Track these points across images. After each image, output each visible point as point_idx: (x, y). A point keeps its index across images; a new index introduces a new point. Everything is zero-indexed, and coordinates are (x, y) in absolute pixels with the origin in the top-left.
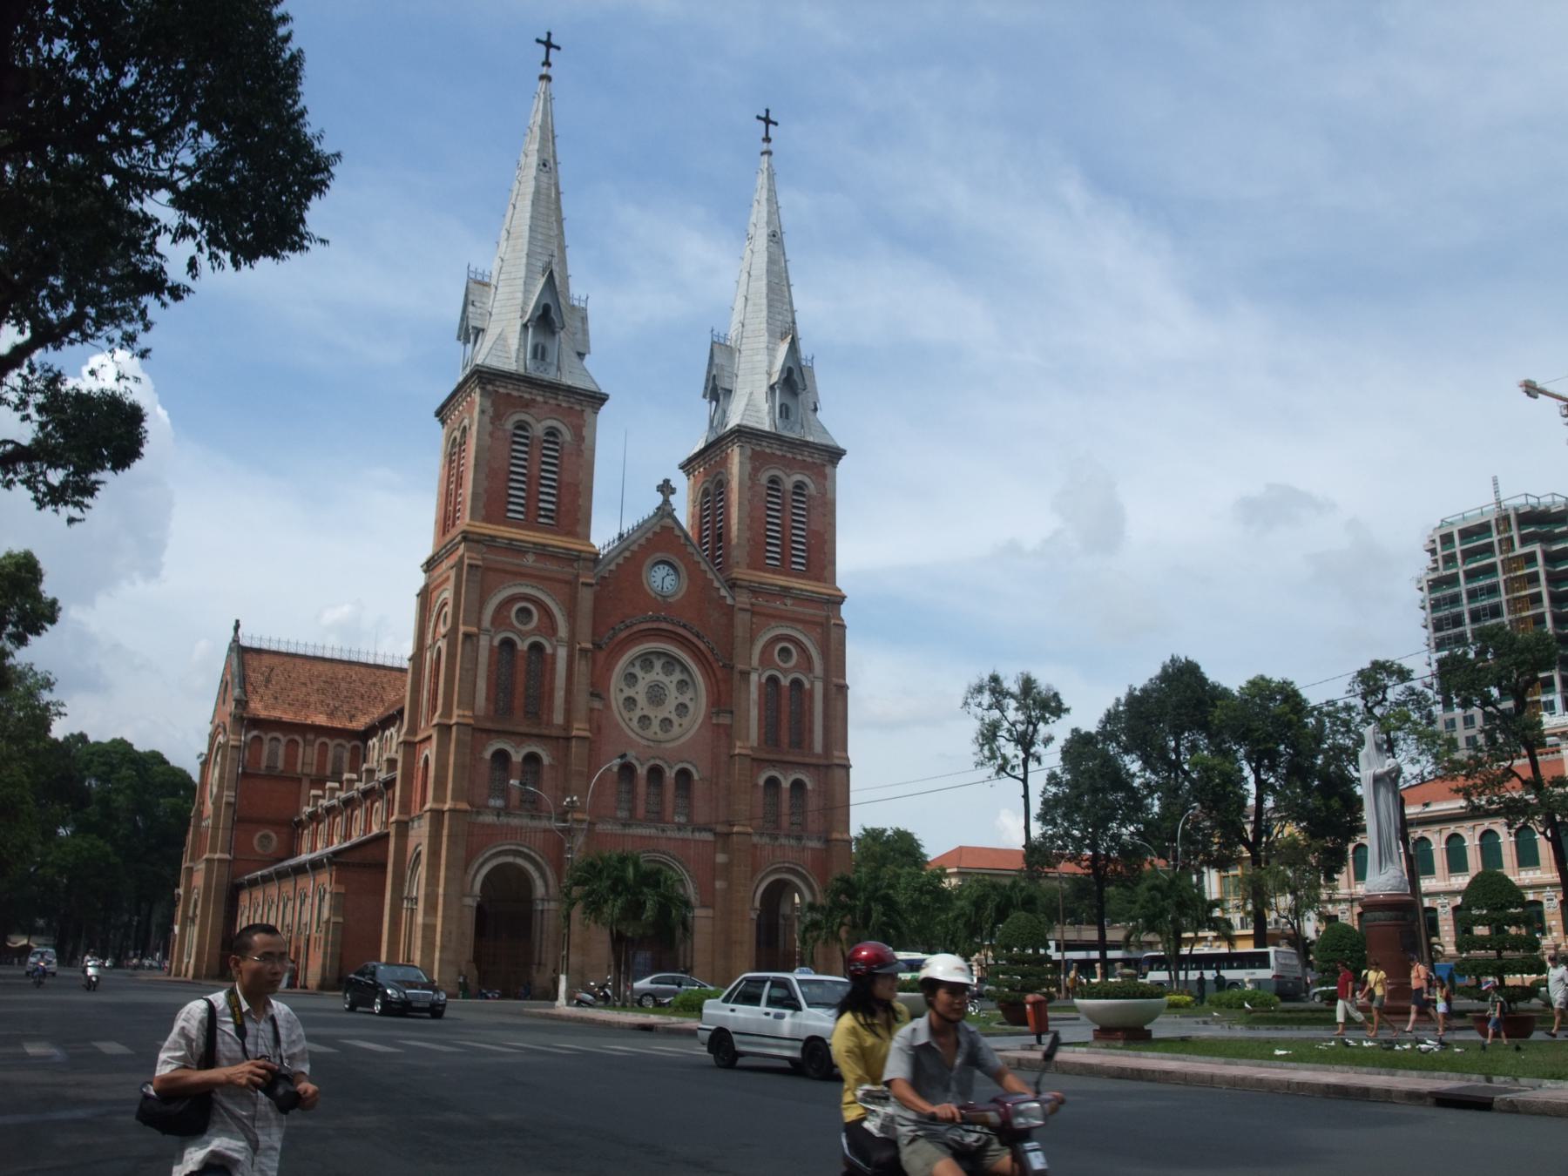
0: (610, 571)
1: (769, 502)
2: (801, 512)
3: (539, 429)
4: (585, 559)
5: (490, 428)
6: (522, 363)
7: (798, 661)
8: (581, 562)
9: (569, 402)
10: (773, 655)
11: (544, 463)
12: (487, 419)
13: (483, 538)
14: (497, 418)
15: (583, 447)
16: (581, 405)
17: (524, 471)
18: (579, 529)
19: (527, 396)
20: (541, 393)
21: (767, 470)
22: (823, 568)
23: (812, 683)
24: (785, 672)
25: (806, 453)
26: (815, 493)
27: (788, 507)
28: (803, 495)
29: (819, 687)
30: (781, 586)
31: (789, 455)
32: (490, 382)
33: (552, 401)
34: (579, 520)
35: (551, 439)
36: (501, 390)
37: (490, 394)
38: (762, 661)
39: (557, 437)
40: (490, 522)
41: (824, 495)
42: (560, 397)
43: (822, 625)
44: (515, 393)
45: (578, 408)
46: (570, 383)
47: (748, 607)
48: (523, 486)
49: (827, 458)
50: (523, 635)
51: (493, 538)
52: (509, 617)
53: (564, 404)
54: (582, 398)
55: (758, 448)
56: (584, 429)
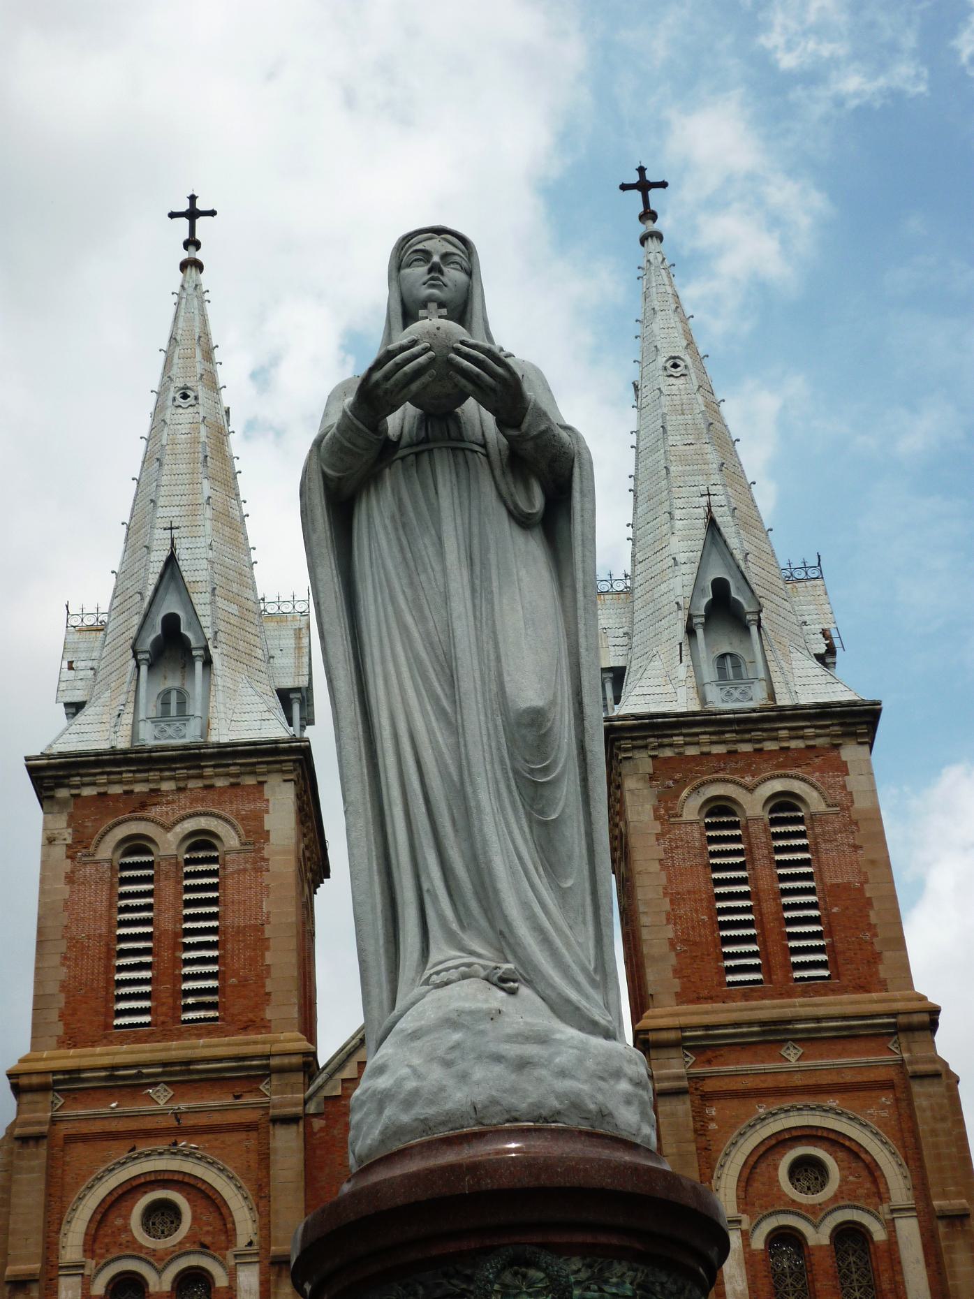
0: (344, 1080)
1: (714, 854)
2: (799, 856)
3: (169, 843)
4: (281, 1070)
5: (67, 865)
6: (125, 731)
7: (844, 1180)
8: (274, 1077)
9: (228, 775)
10: (774, 1181)
11: (189, 903)
12: (59, 851)
13: (51, 1078)
14: (80, 846)
15: (266, 854)
16: (253, 773)
17: (149, 929)
18: (269, 1014)
19: (139, 788)
20: (167, 774)
21: (696, 789)
22: (876, 958)
23: (890, 1227)
24: (814, 1214)
25: (783, 733)
26: (822, 807)
27: (761, 853)
28: (800, 821)
29: (909, 1230)
30: (762, 1023)
31: (746, 748)
32: (60, 783)
33: (192, 784)
34: (268, 994)
35: (201, 855)
36: (87, 792)
37: (63, 804)
38: (745, 1199)
39: (214, 848)
40: (75, 1046)
41: (846, 808)
42: (208, 772)
43: (887, 1085)
44: (117, 790)
45: (250, 781)
46: (224, 740)
47: (685, 1083)
48: (148, 959)
49: (837, 730)
50: (159, 1261)
51: (73, 1074)
52: (126, 1228)
53: (220, 783)
54: (255, 760)
55: (668, 753)
56: (266, 816)
